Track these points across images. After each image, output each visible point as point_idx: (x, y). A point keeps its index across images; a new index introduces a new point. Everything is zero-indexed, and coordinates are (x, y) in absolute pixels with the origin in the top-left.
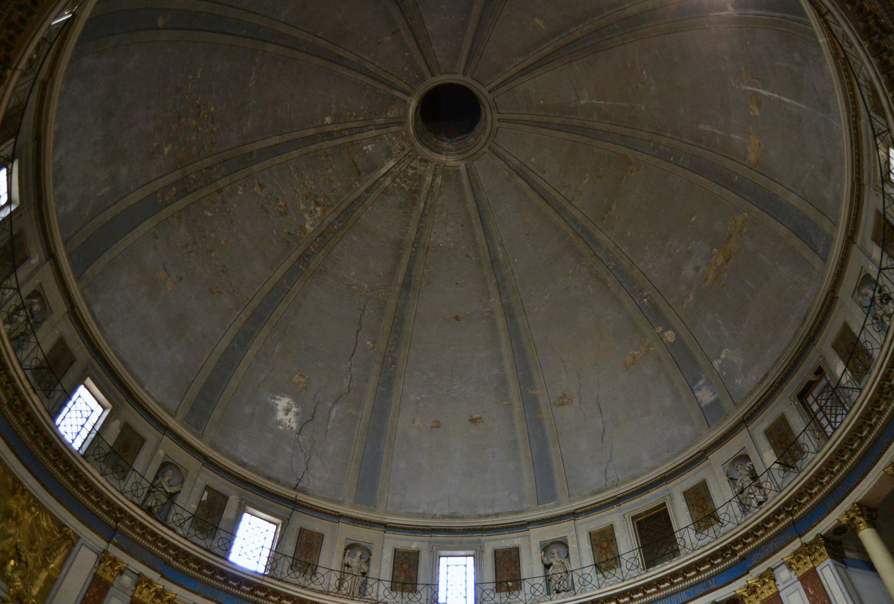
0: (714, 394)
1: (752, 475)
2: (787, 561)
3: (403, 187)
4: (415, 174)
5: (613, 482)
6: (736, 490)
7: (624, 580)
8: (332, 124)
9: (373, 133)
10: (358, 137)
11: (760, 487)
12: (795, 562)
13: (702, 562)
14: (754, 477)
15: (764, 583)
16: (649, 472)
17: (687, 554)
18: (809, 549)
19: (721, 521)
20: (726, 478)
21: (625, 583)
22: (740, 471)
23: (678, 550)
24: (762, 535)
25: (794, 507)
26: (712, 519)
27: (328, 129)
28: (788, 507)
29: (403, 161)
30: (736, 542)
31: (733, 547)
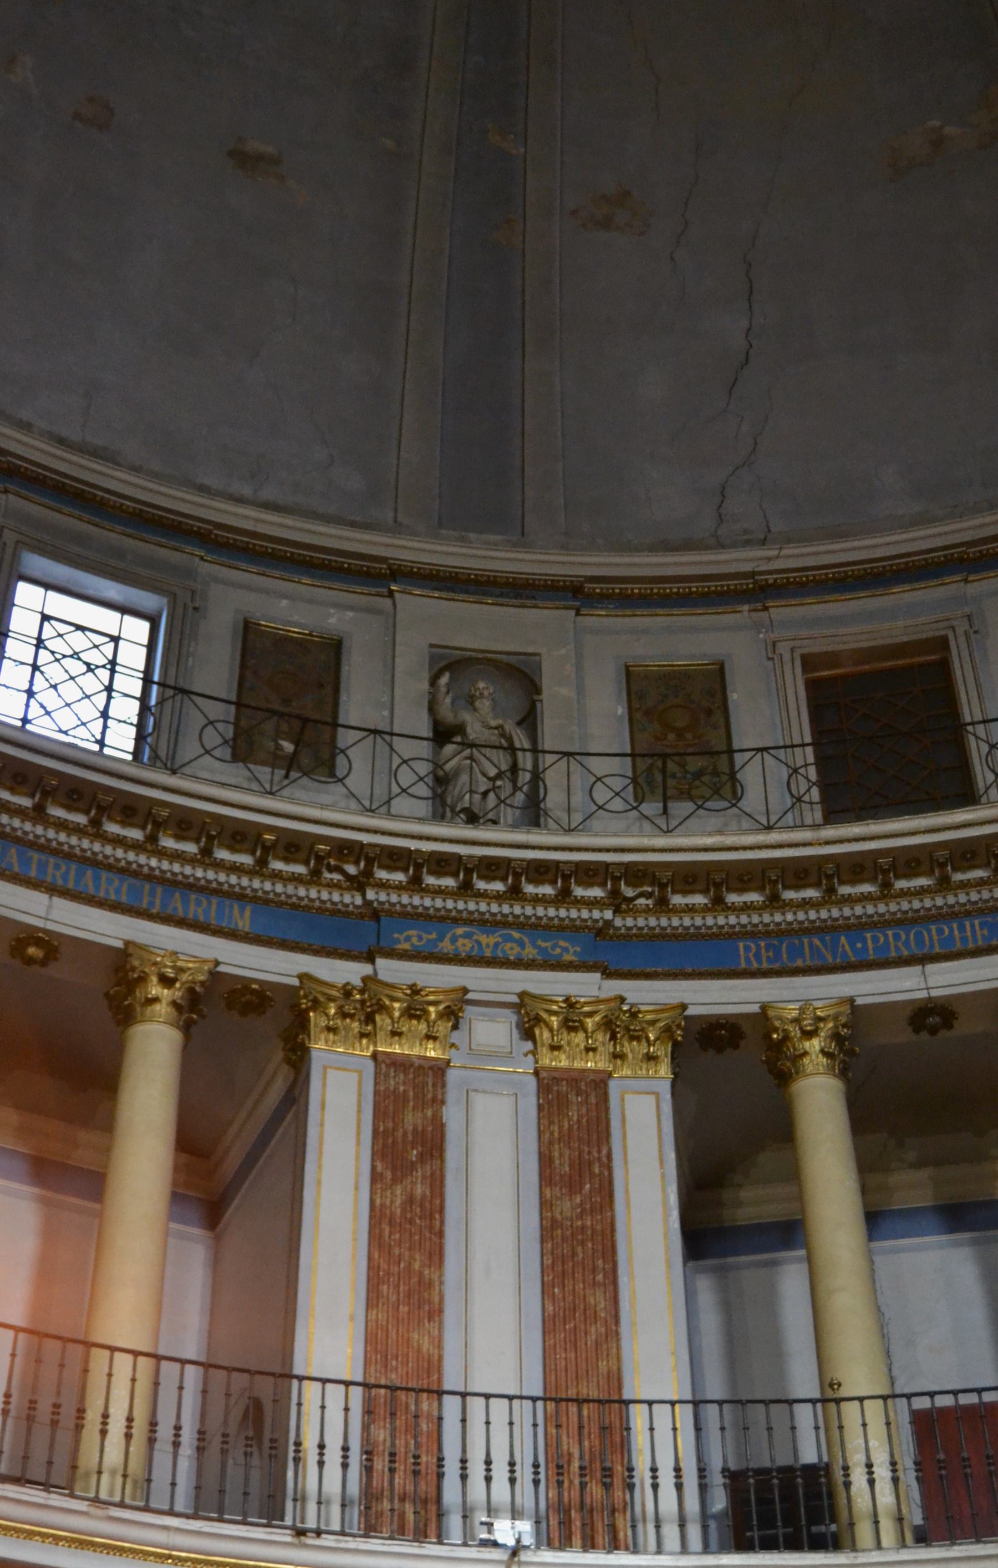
7: (769, 828)
21: (774, 837)
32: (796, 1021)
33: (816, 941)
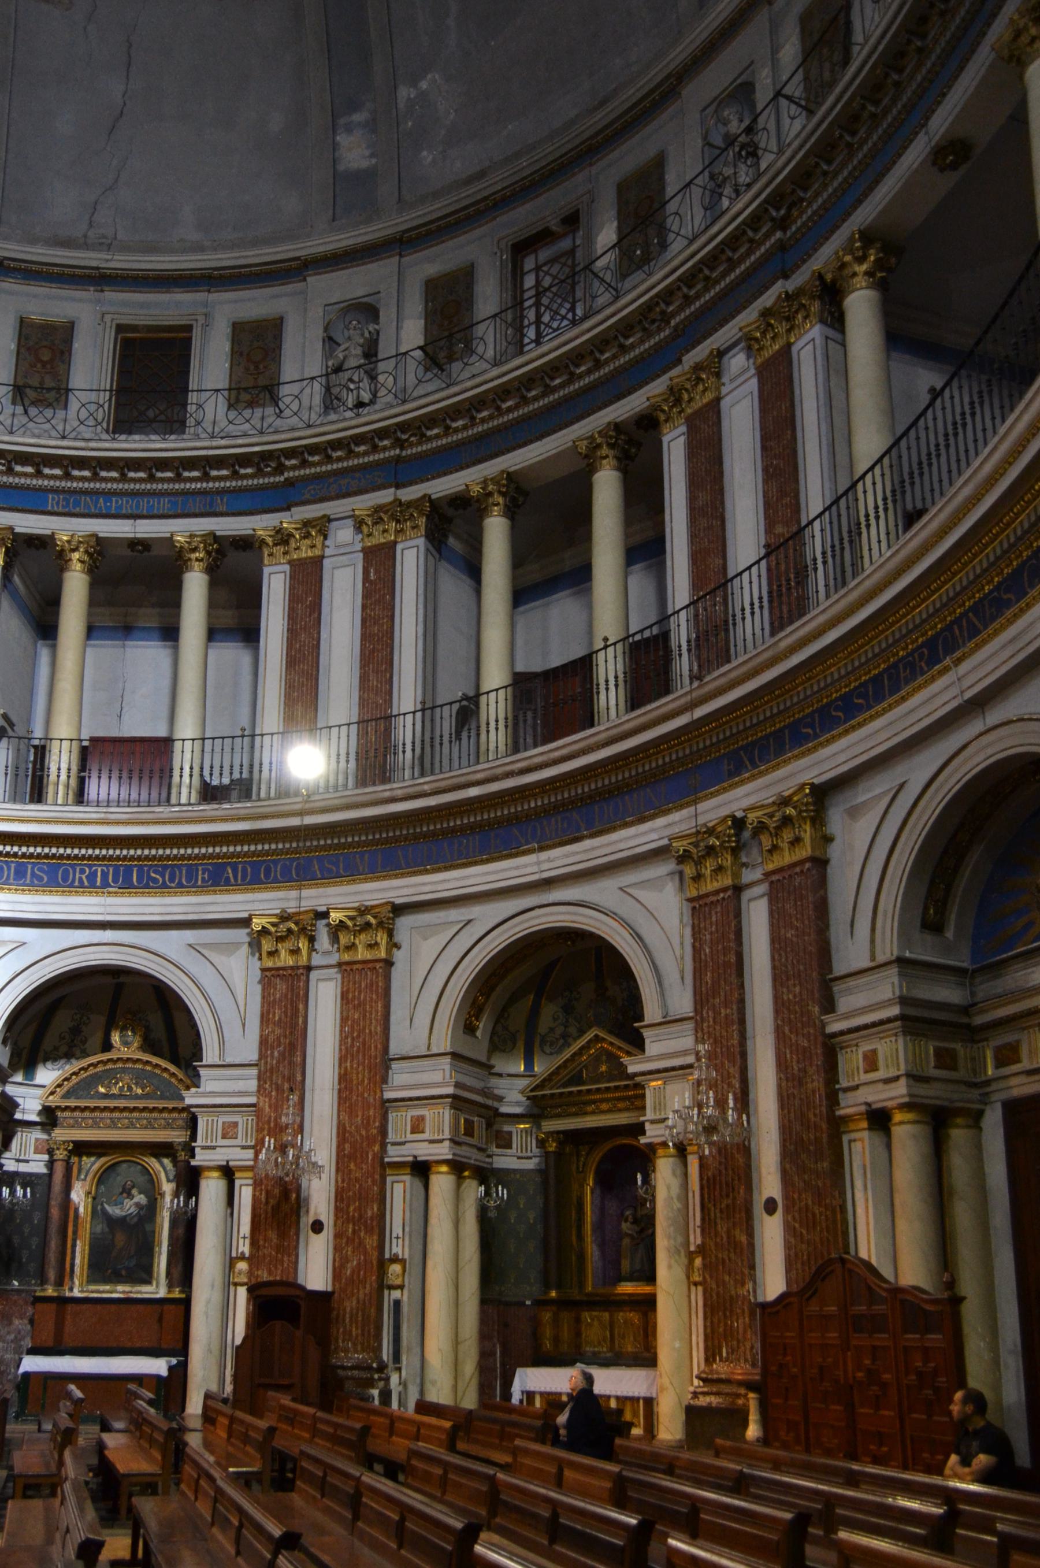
0: (372, 156)
1: (369, 348)
2: (358, 516)
5: (104, 237)
6: (330, 363)
11: (373, 377)
12: (370, 523)
13: (219, 462)
14: (371, 353)
15: (307, 536)
16: (184, 251)
17: (197, 437)
18: (401, 512)
19: (280, 404)
20: (320, 333)
22: (351, 331)
23: (183, 424)
24: (339, 459)
25: (411, 436)
26: (268, 396)
28: (403, 432)
30: (290, 453)
31: (283, 459)
32: (69, 542)
33: (88, 499)
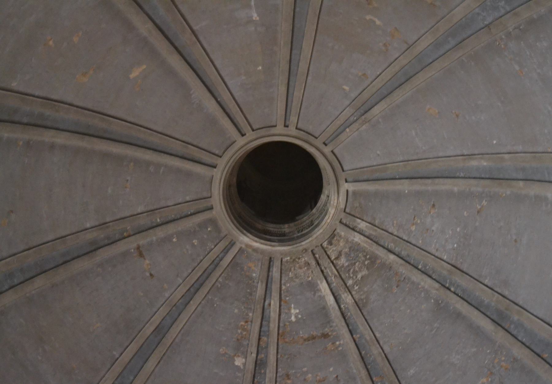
3: (362, 277)
4: (347, 255)
8: (246, 358)
9: (274, 303)
10: (273, 326)
27: (251, 366)
29: (325, 268)
